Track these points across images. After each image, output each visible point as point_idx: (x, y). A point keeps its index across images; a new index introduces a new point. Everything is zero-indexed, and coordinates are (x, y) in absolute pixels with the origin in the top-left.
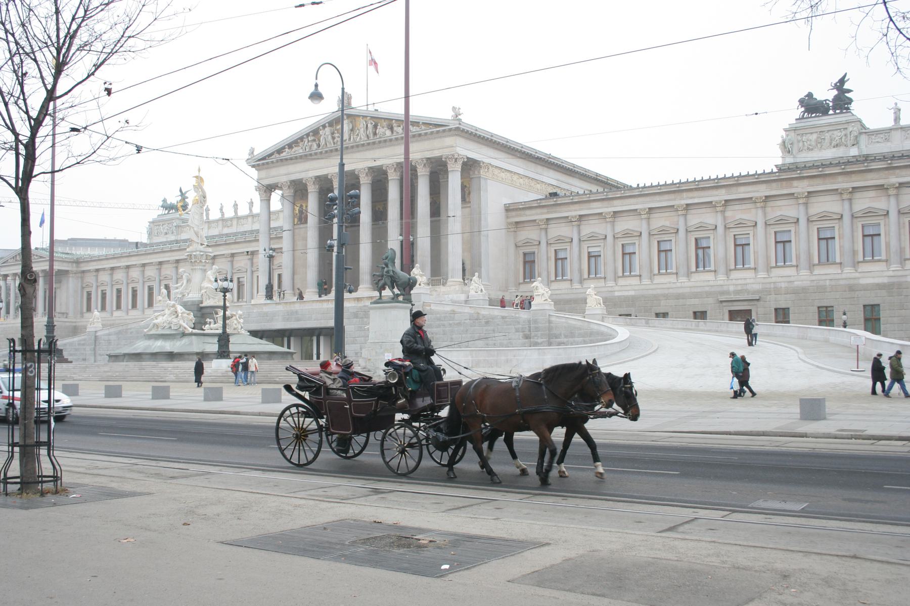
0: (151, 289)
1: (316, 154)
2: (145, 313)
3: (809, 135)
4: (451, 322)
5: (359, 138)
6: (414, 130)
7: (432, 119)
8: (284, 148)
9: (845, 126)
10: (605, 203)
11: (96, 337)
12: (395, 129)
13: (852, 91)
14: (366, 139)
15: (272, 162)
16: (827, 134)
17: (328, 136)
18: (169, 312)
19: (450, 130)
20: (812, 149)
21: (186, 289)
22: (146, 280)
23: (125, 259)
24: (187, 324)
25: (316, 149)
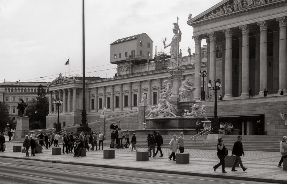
0: (135, 96)
1: (231, 15)
2: (123, 110)
5: (260, 3)
8: (210, 13)
11: (105, 121)
14: (265, 3)
15: (203, 22)
17: (238, 3)
21: (169, 92)
22: (123, 92)
23: (112, 82)
24: (173, 112)
25: (232, 12)
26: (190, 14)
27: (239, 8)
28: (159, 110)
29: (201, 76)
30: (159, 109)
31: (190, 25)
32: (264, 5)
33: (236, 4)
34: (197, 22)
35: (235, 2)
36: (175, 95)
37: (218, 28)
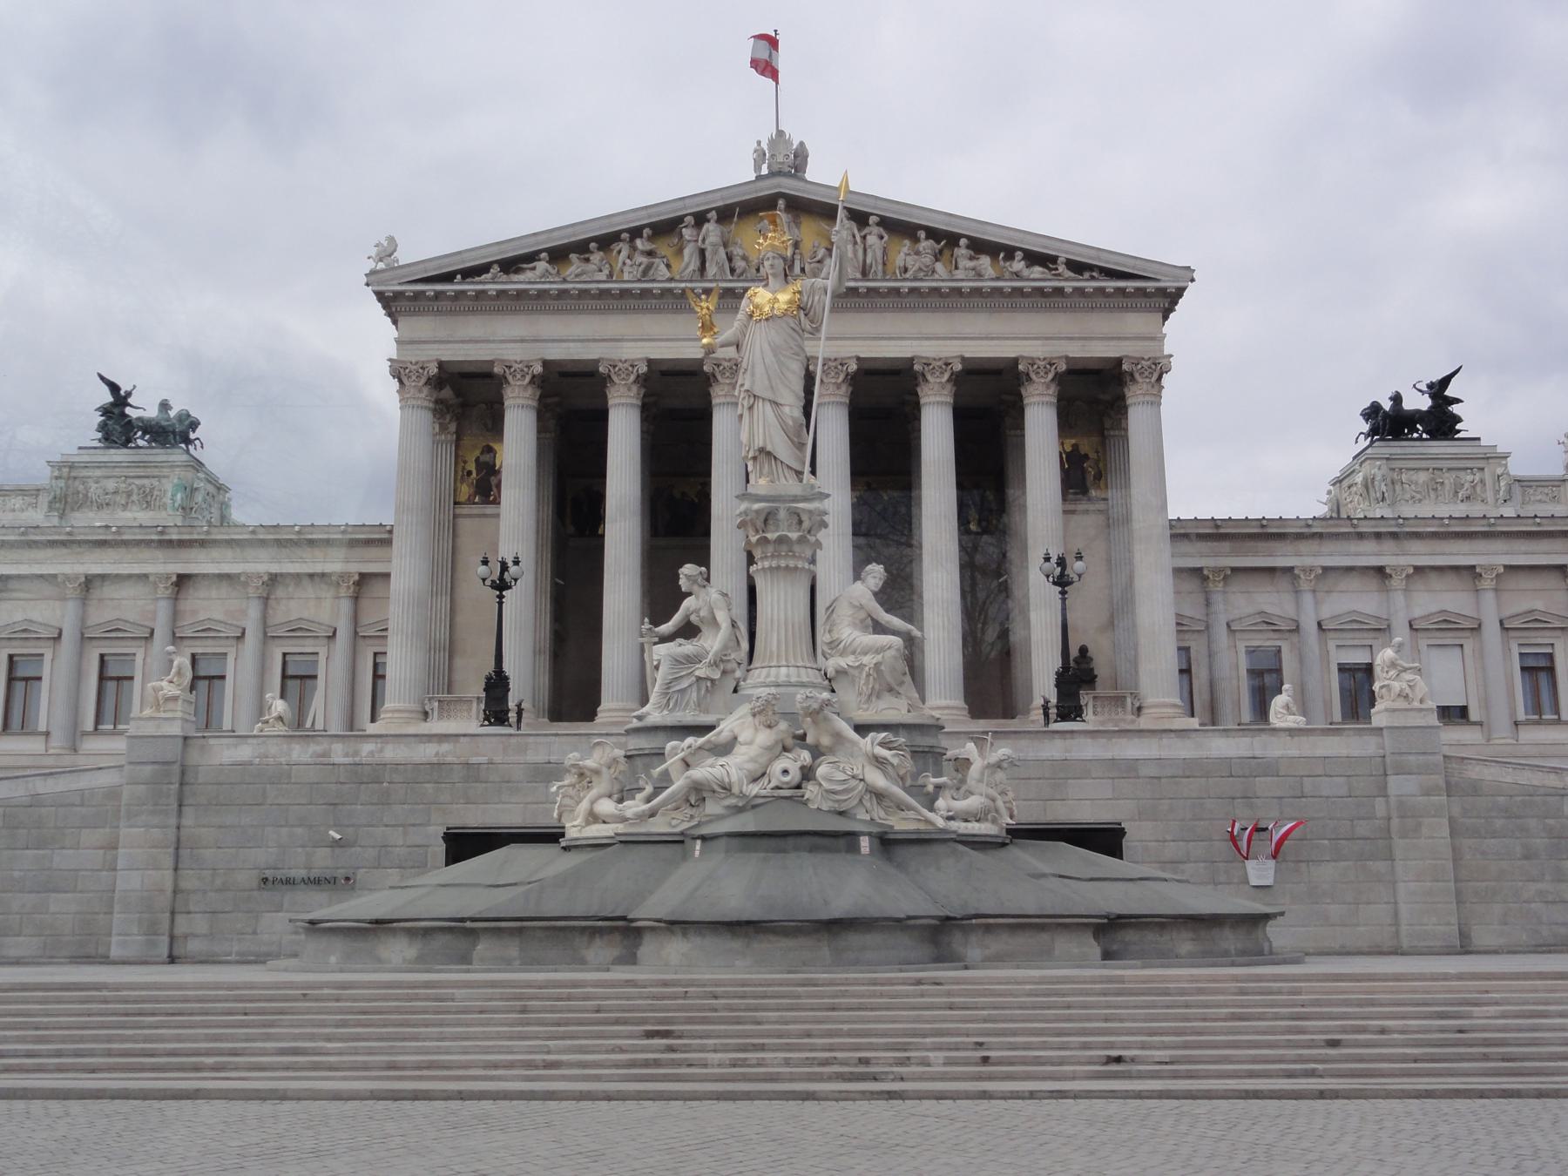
3: (1412, 472)
4: (1551, 822)
6: (1032, 276)
7: (1104, 255)
8: (531, 257)
9: (1480, 464)
10: (1389, 545)
12: (964, 263)
13: (1462, 401)
14: (859, 276)
15: (480, 295)
16: (1447, 475)
17: (714, 245)
18: (765, 737)
19: (1162, 292)
20: (1420, 501)
26: (391, 239)
27: (711, 270)
28: (751, 766)
29: (488, 582)
30: (752, 760)
31: (379, 300)
32: (860, 284)
33: (692, 244)
34: (439, 287)
35: (687, 237)
36: (803, 671)
37: (572, 345)
